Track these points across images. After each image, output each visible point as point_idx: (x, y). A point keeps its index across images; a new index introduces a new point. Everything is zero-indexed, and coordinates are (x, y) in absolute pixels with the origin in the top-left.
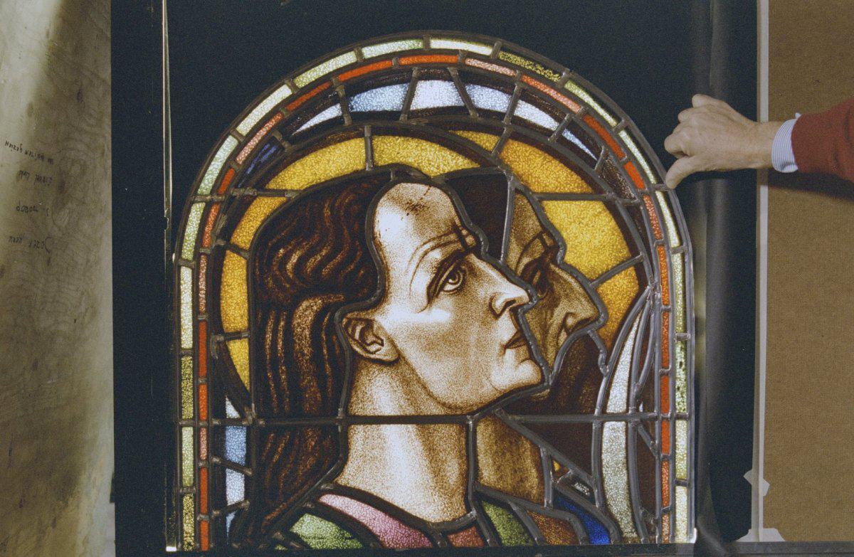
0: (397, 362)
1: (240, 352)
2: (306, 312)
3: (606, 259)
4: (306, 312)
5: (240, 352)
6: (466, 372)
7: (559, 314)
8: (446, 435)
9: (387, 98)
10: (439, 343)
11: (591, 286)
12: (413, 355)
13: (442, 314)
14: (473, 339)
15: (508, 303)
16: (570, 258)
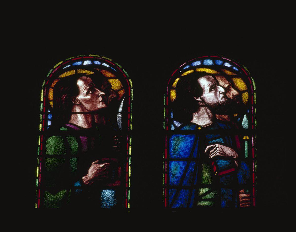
0: (80, 105)
1: (51, 103)
2: (64, 96)
3: (119, 88)
4: (64, 96)
5: (51, 103)
6: (93, 106)
7: (110, 96)
8: (89, 116)
9: (79, 63)
10: (87, 101)
11: (116, 91)
12: (84, 103)
13: (89, 97)
14: (94, 100)
15: (101, 95)
16: (112, 88)
